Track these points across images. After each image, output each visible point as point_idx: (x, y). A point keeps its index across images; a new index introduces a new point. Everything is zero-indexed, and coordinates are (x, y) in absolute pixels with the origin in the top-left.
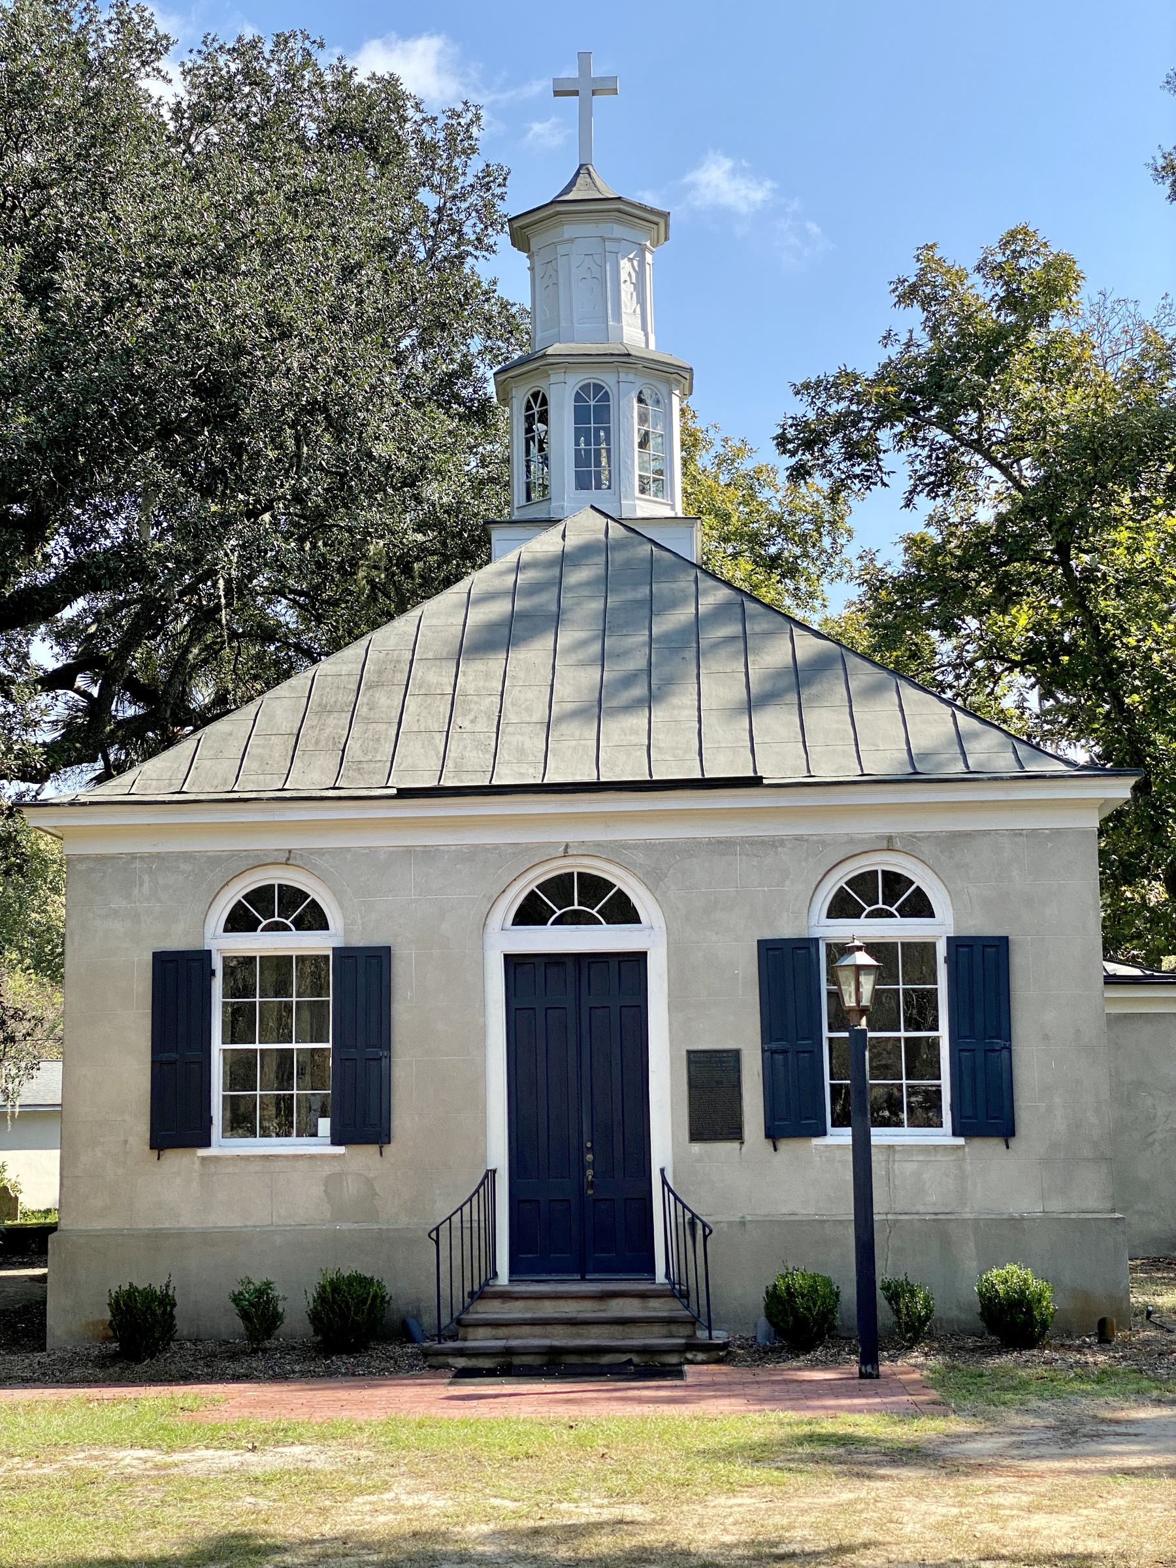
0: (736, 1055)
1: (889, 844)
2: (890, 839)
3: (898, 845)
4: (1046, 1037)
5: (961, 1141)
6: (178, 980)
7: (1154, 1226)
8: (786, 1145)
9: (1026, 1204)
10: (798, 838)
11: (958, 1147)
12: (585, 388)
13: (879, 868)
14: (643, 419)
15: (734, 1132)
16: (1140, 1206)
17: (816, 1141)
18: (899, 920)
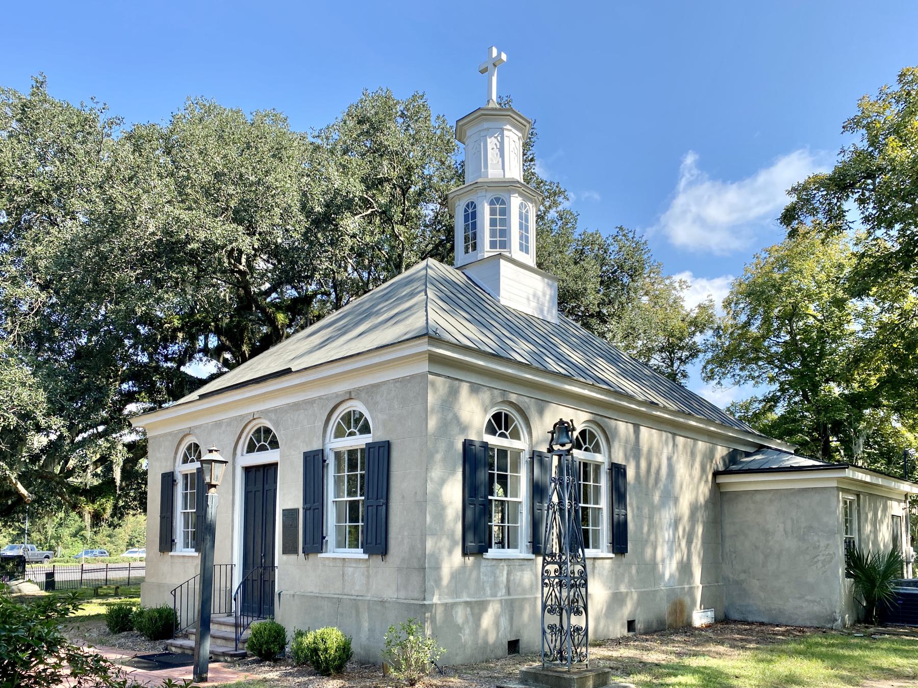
0: (297, 510)
1: (350, 396)
2: (350, 393)
3: (353, 395)
4: (403, 497)
5: (366, 556)
6: (168, 480)
7: (816, 608)
8: (311, 557)
9: (390, 594)
10: (320, 398)
11: (367, 560)
12: (468, 206)
13: (351, 409)
14: (493, 212)
15: (296, 552)
16: (808, 597)
17: (320, 555)
18: (358, 436)
